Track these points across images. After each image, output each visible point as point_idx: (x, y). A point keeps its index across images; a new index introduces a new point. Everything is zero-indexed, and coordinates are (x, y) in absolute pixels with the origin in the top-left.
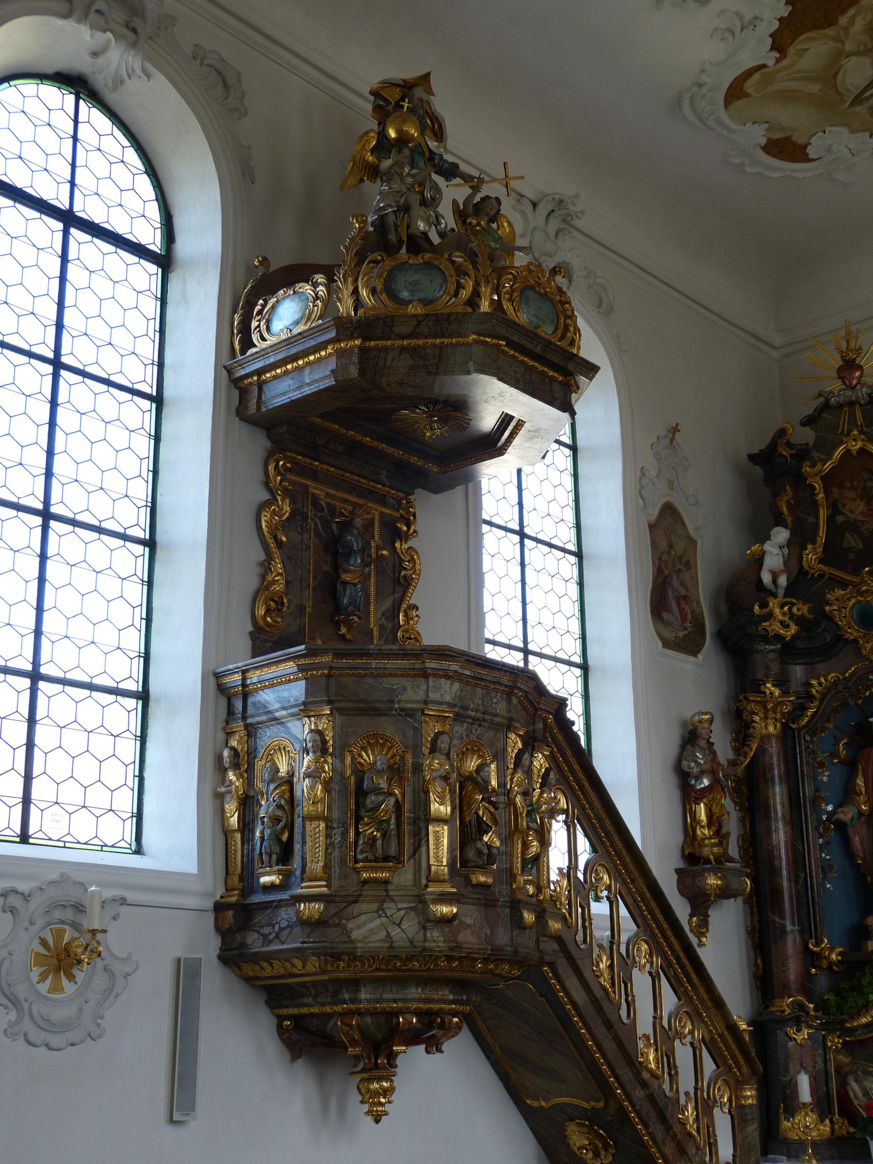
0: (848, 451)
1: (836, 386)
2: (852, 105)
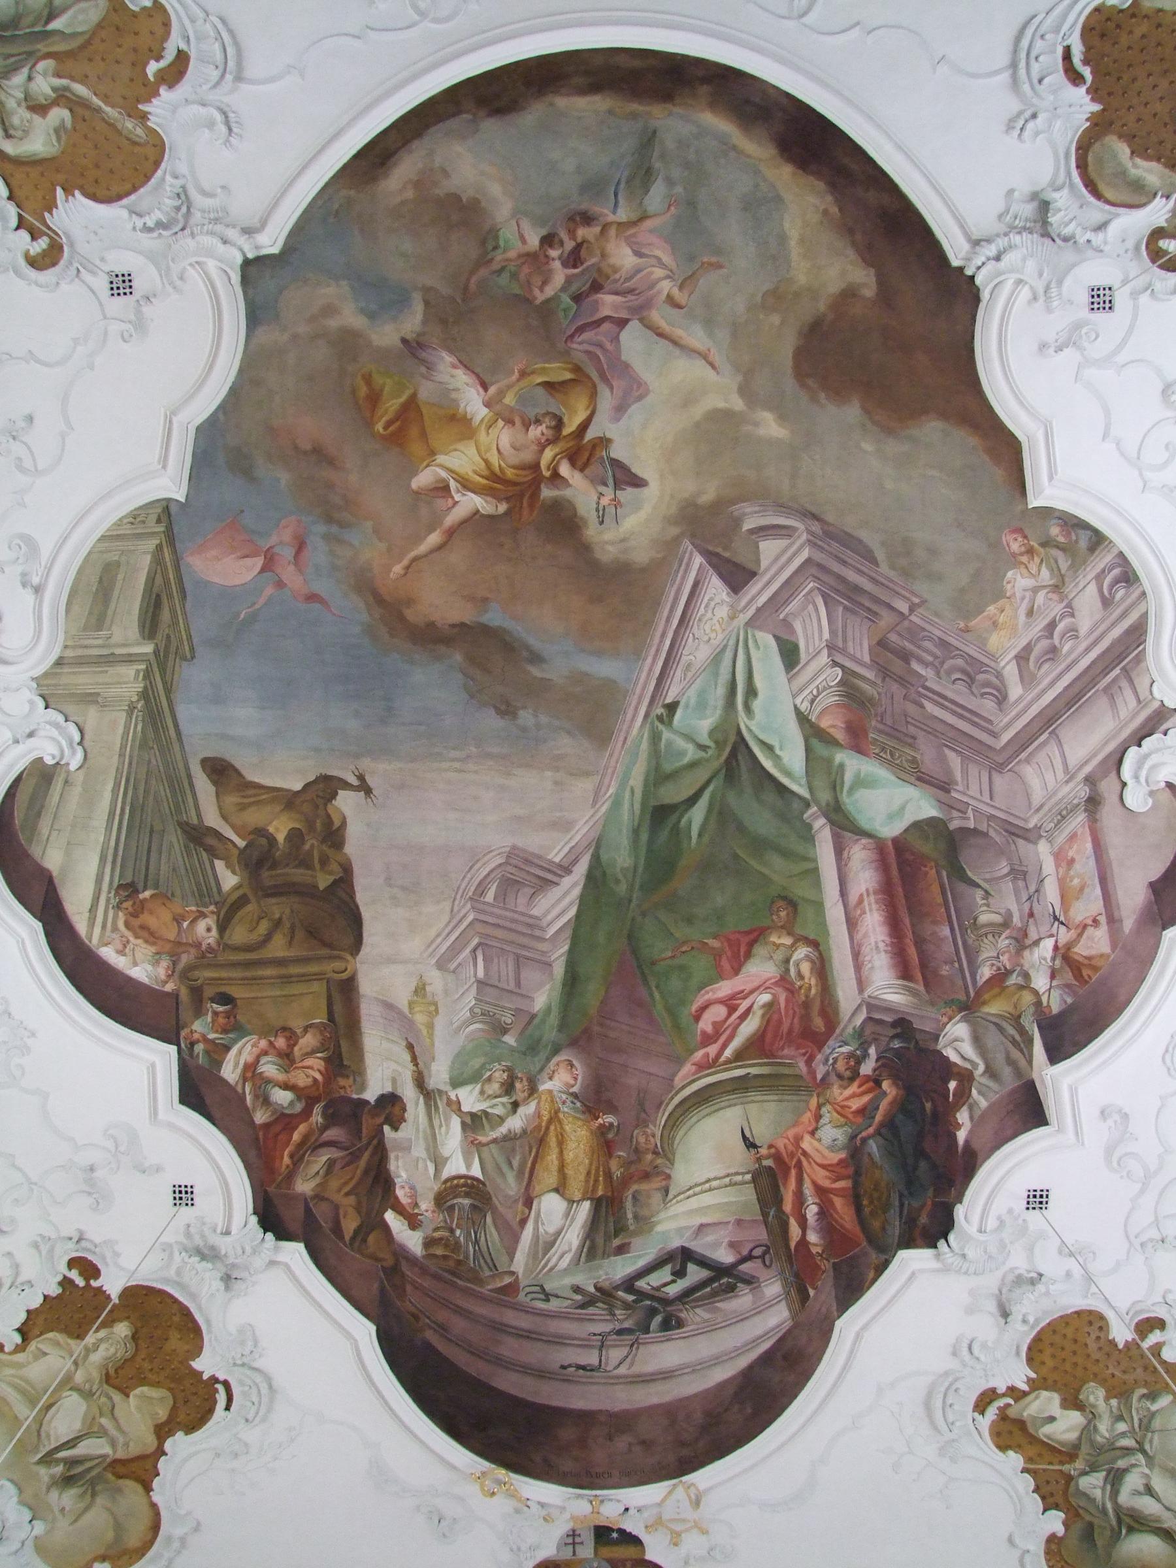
2: (41, 1461)
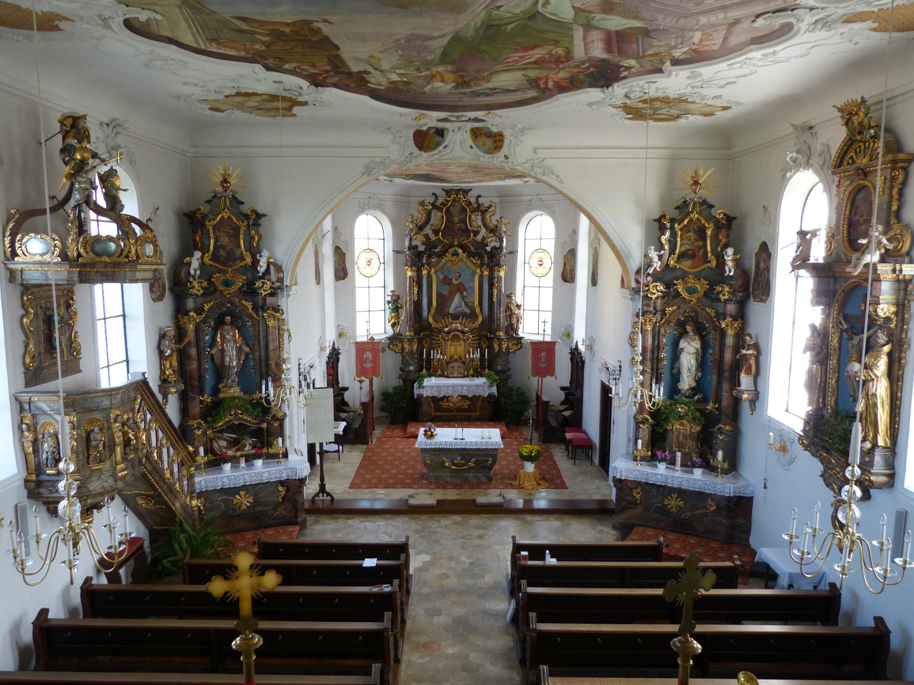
0: (223, 217)
1: (220, 189)
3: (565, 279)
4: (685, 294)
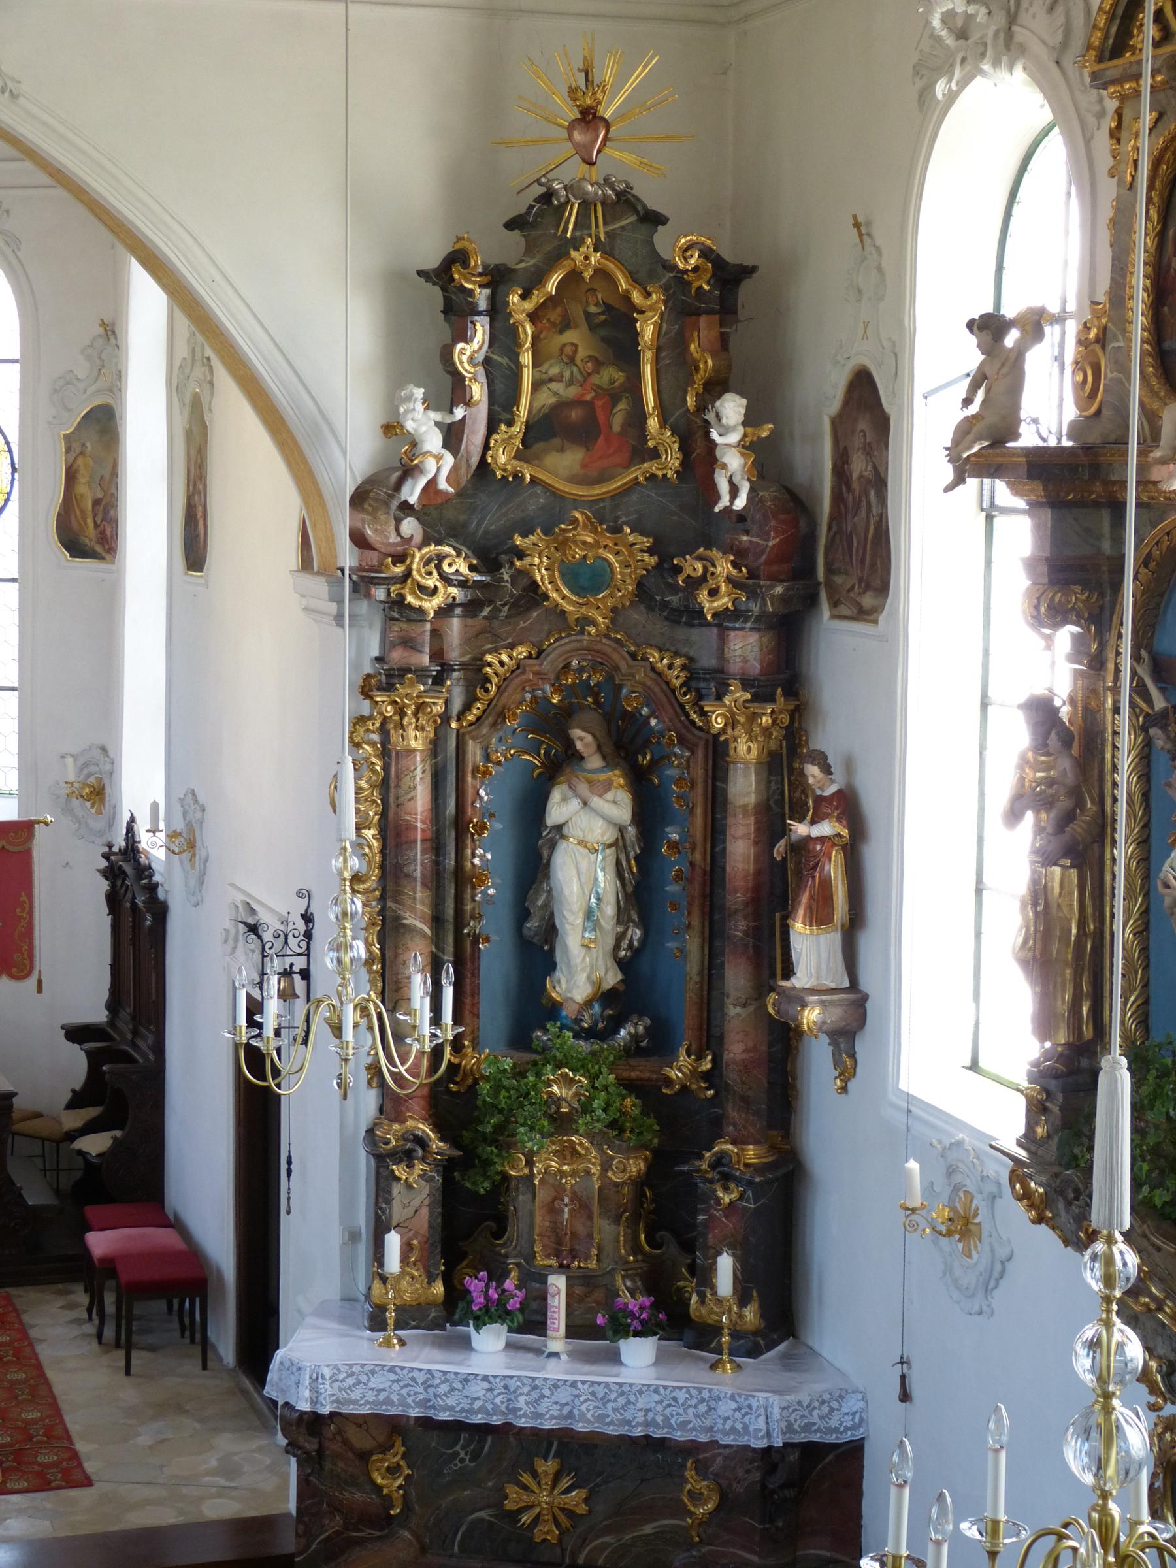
3: (74, 545)
4: (559, 594)
